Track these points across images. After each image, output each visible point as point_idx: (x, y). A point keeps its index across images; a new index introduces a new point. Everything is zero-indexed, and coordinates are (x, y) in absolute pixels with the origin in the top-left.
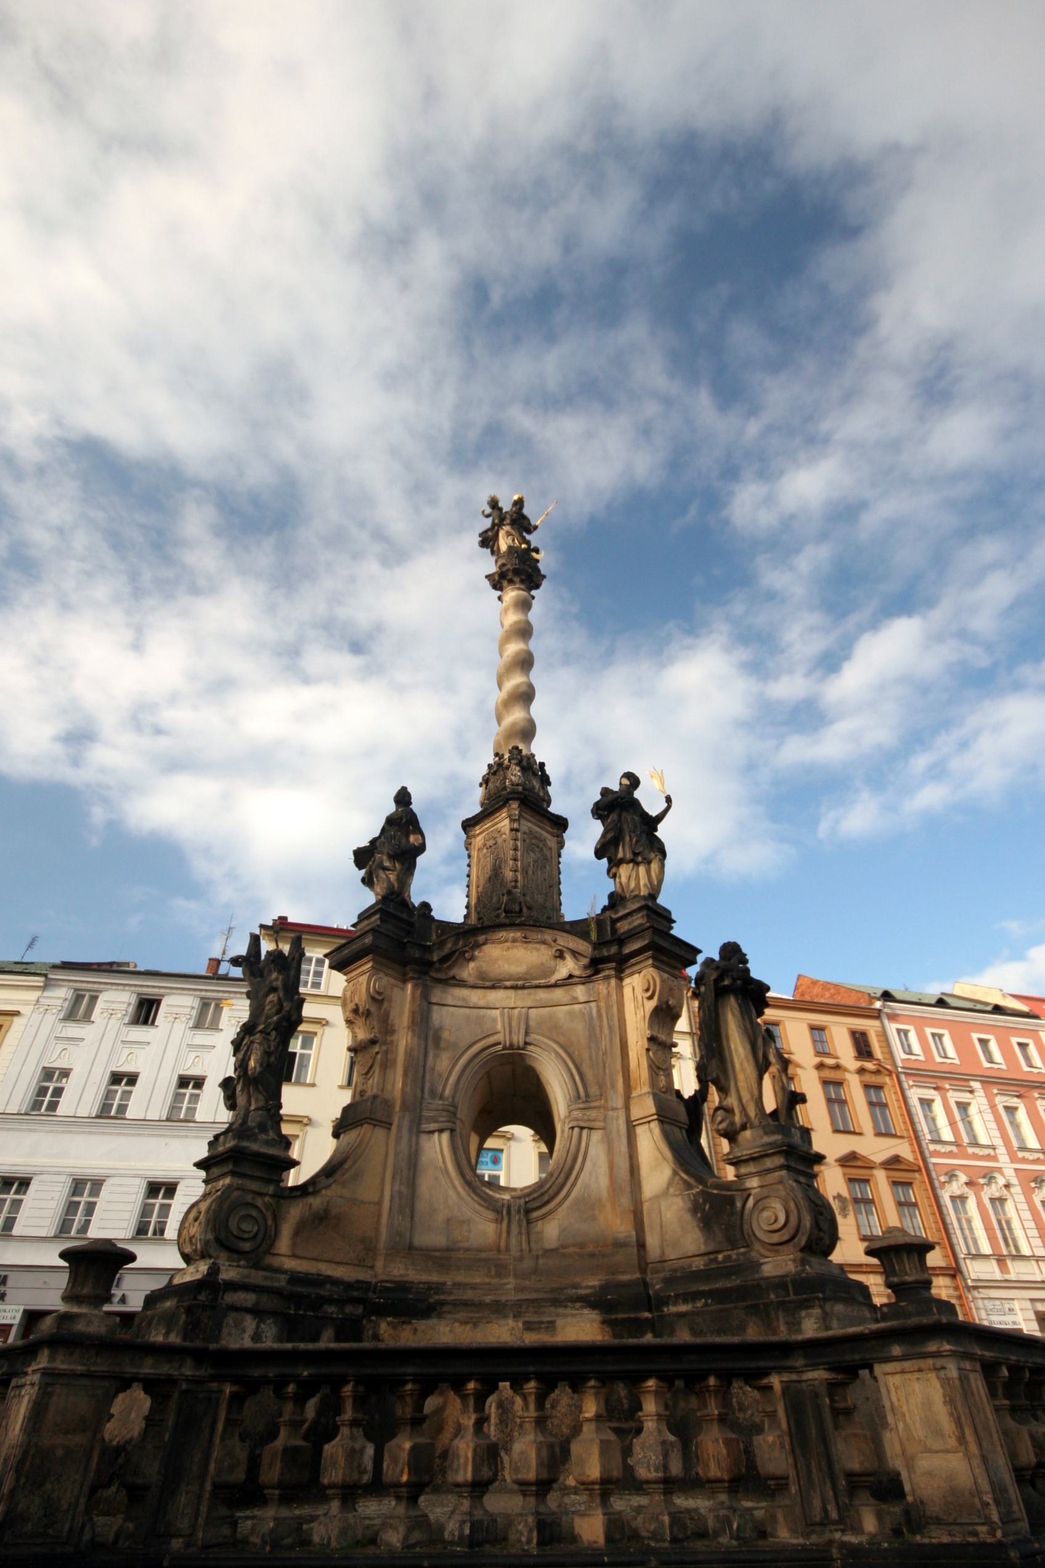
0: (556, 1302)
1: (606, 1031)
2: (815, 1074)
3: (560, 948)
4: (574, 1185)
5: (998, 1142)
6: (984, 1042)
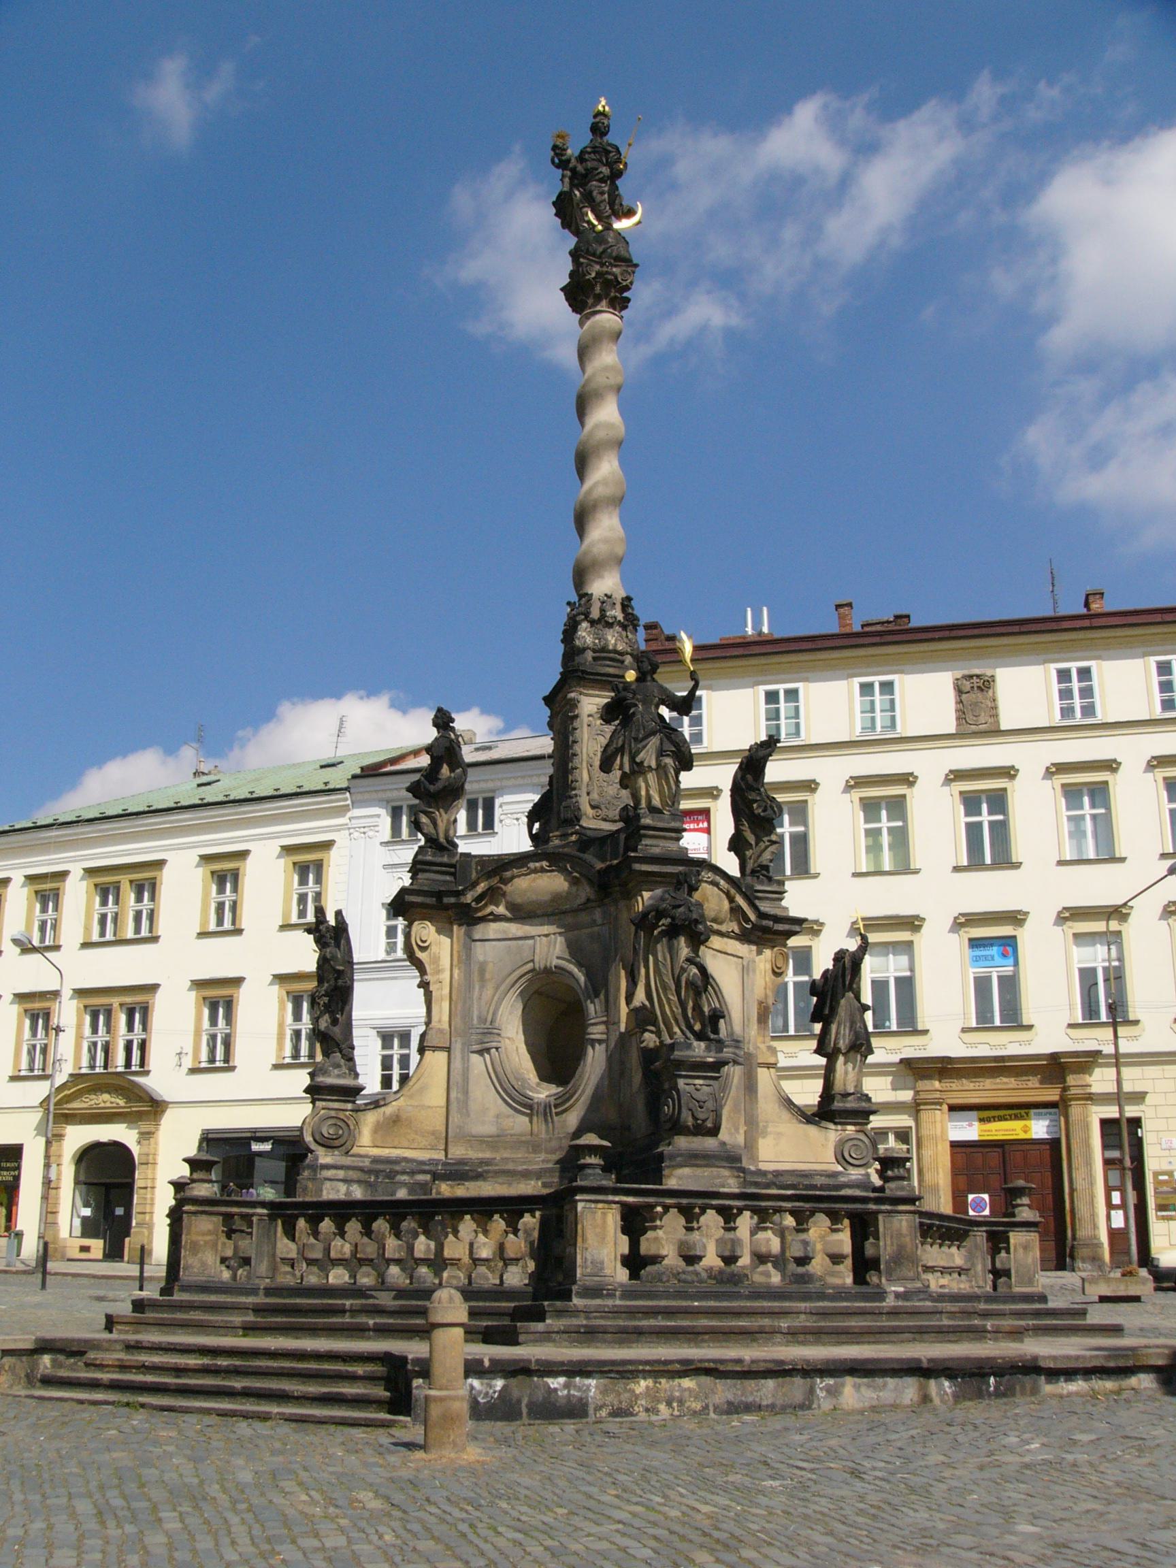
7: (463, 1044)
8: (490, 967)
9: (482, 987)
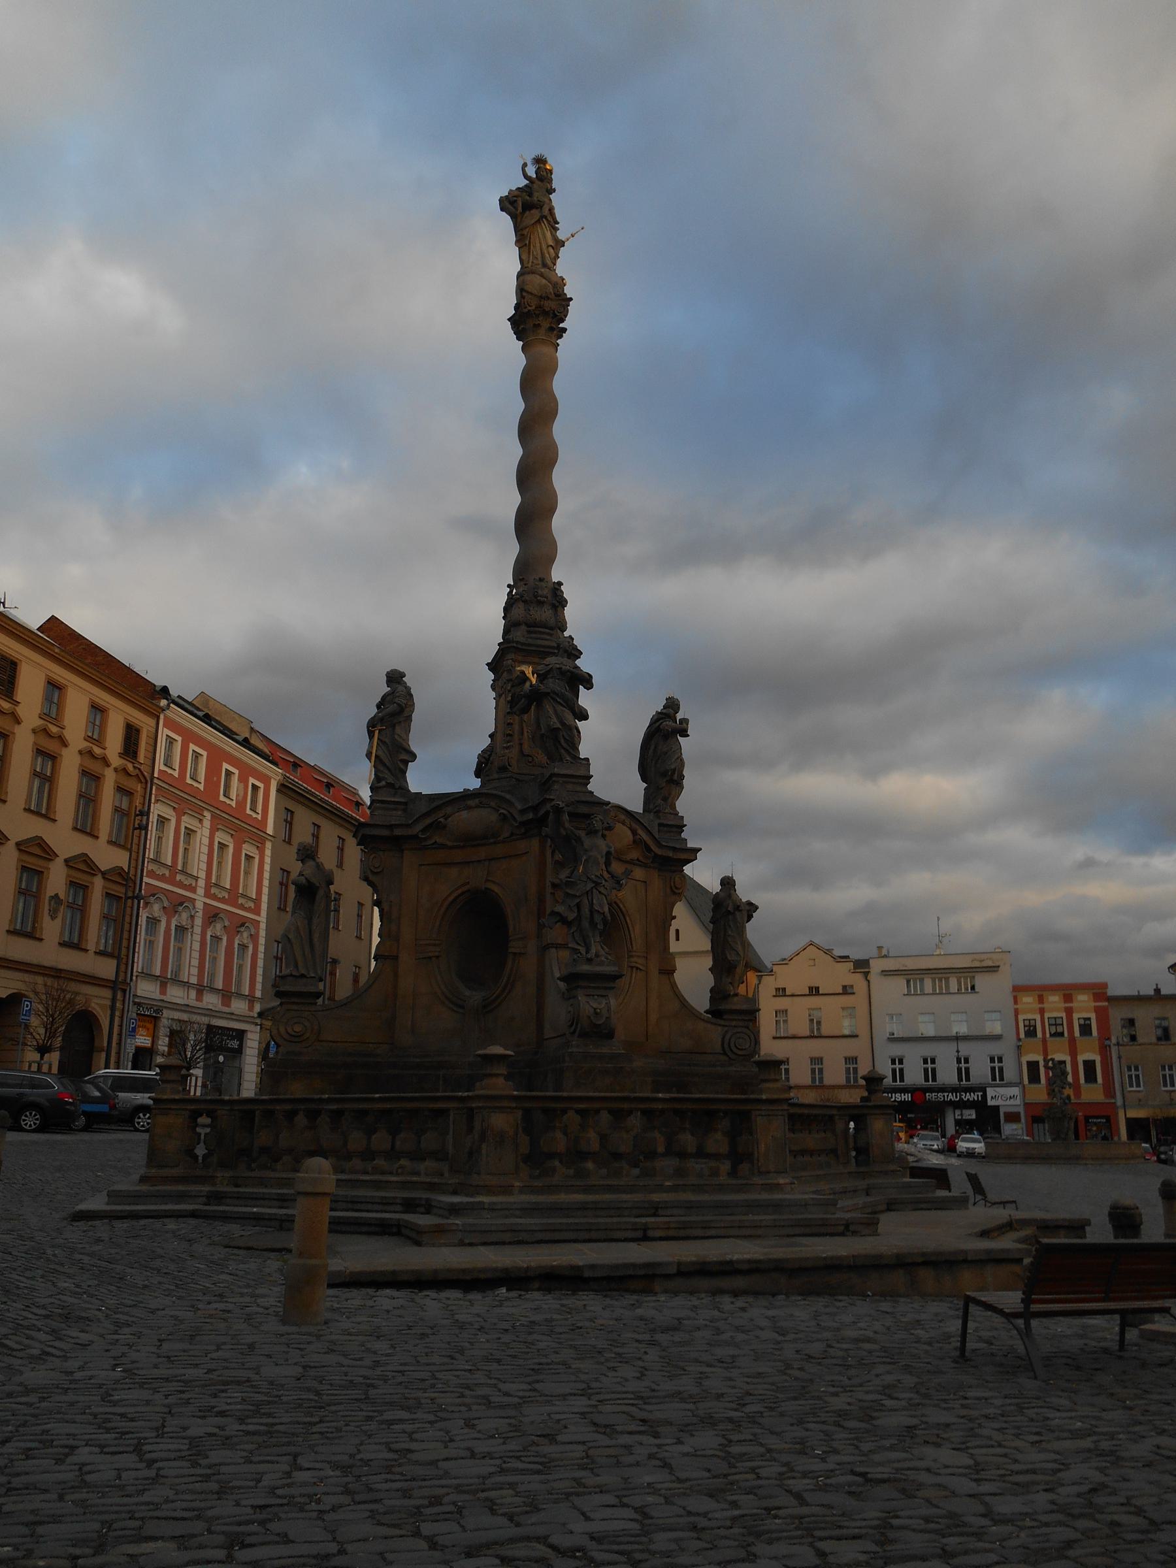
2: (77, 760)
5: (202, 875)
6: (228, 773)
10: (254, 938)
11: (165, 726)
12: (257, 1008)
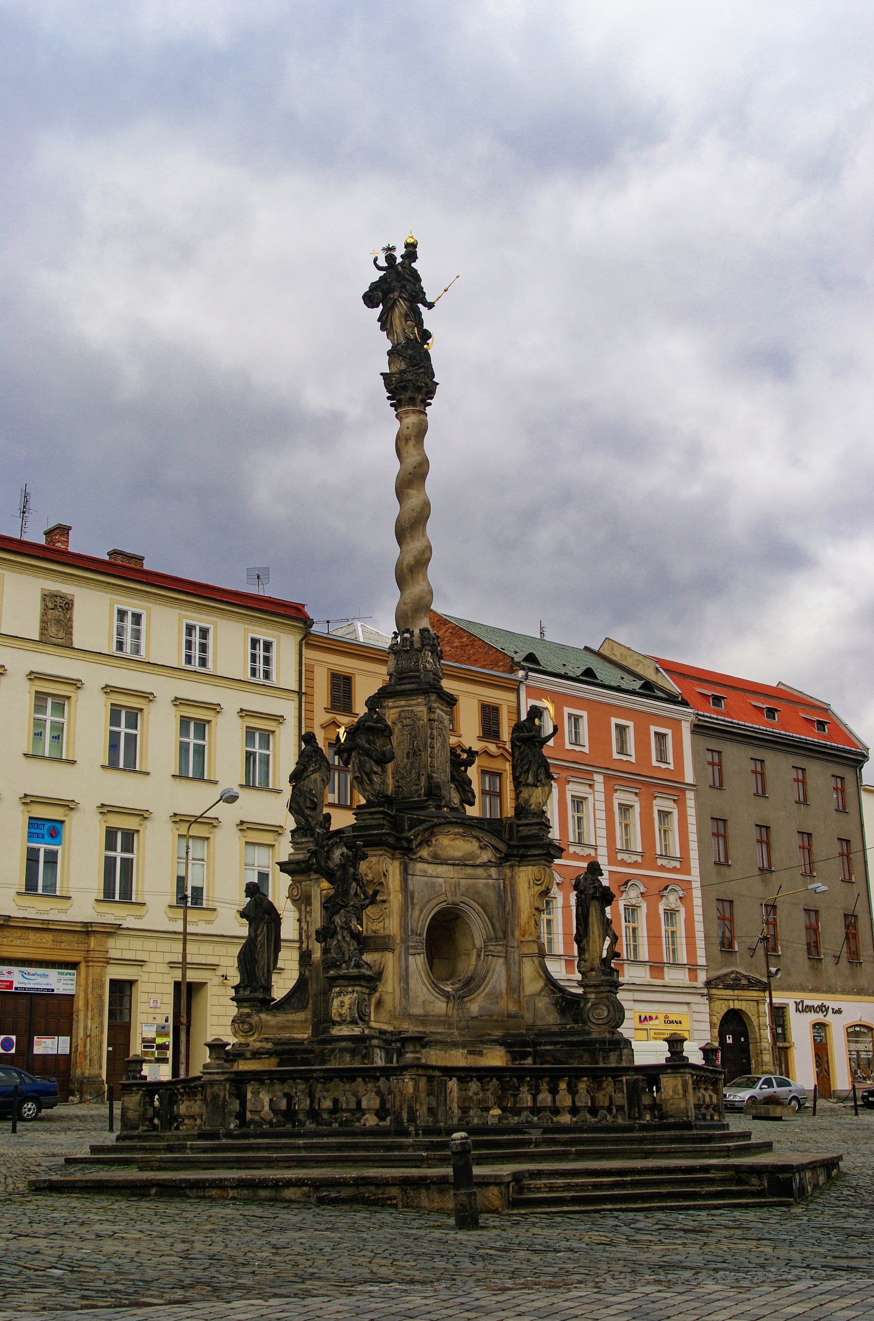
0: (482, 1042)
1: (510, 899)
3: (486, 843)
4: (487, 986)
5: (602, 842)
6: (621, 729)
7: (405, 949)
8: (416, 894)
9: (413, 909)
10: (685, 899)
11: (528, 696)
12: (702, 976)
